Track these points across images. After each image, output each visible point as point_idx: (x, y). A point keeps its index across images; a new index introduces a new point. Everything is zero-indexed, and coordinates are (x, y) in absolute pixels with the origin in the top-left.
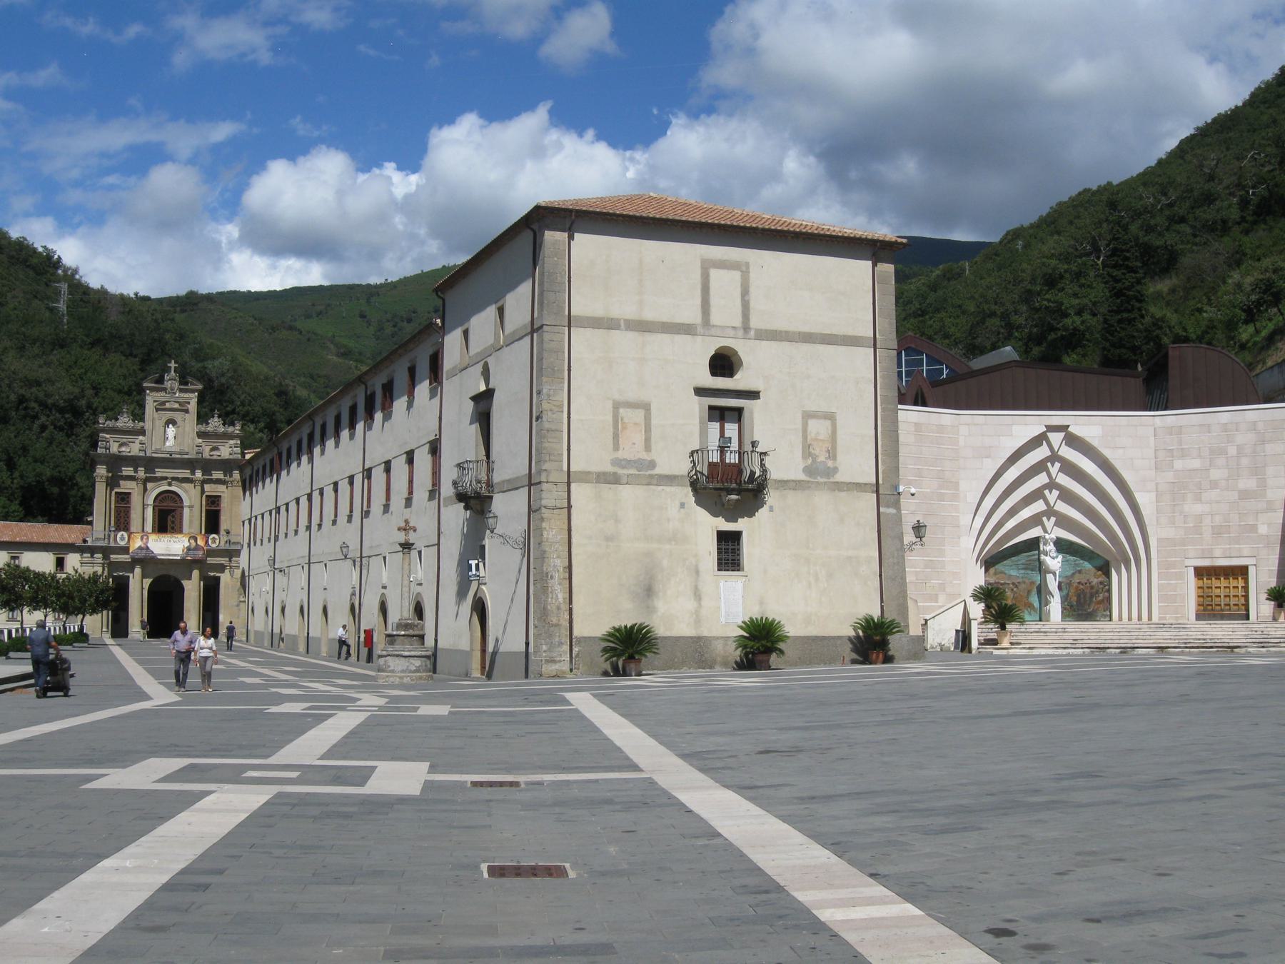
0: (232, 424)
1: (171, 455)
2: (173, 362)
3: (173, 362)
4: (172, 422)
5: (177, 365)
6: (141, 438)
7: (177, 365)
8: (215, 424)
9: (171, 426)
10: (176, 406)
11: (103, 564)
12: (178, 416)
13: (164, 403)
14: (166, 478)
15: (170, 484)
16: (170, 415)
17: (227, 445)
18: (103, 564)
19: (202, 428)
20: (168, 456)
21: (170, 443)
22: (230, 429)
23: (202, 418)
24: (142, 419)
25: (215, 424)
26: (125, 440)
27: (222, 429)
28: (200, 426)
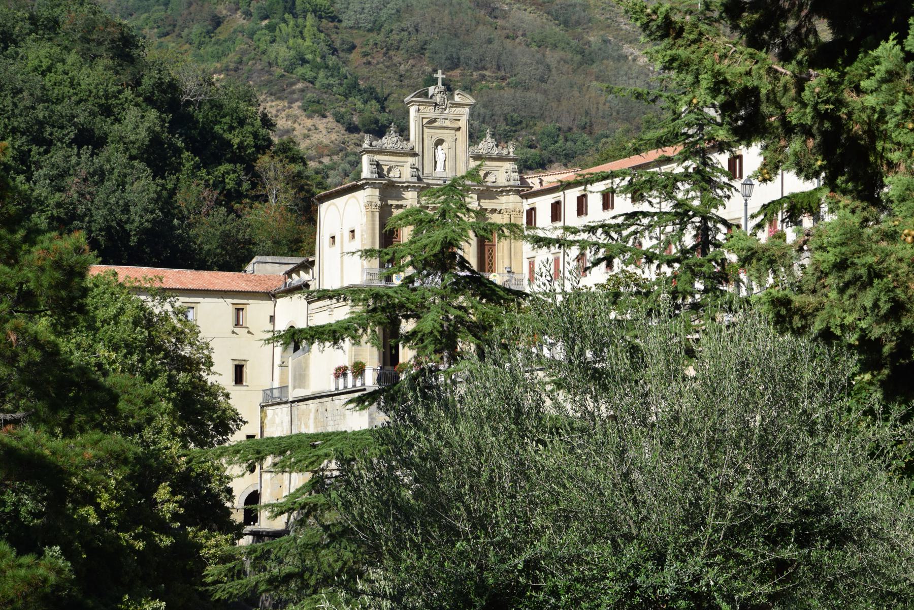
3: (440, 72)
4: (440, 142)
6: (411, 160)
8: (486, 145)
9: (439, 147)
10: (447, 123)
13: (434, 120)
16: (440, 134)
17: (503, 170)
19: (475, 149)
20: (441, 182)
21: (440, 167)
23: (474, 137)
24: (408, 140)
25: (486, 145)
26: (393, 164)
27: (495, 151)
28: (472, 148)
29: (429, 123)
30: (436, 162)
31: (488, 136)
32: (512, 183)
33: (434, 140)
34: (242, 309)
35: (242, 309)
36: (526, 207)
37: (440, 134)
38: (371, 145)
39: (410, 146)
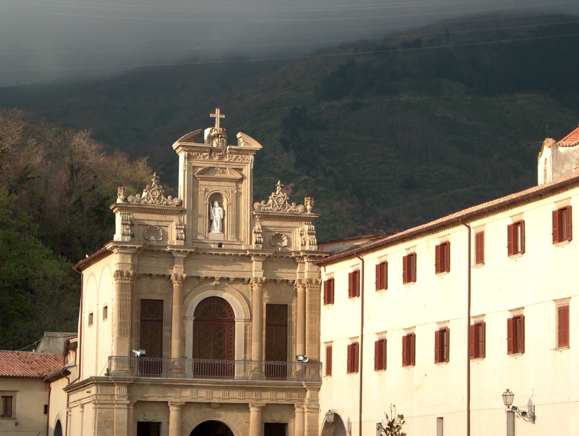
0: (300, 202)
1: (220, 245)
2: (218, 111)
3: (218, 111)
4: (216, 198)
5: (224, 117)
6: (175, 219)
7: (224, 117)
8: (278, 198)
9: (216, 204)
11: (128, 405)
12: (224, 188)
14: (213, 279)
15: (216, 287)
16: (214, 187)
18: (128, 405)
22: (300, 208)
24: (175, 194)
25: (278, 198)
28: (256, 205)
29: (201, 173)
30: (211, 222)
31: (278, 189)
32: (307, 248)
33: (208, 195)
34: (11, 397)
35: (11, 397)
36: (325, 278)
37: (214, 187)
38: (126, 200)
39: (176, 201)
